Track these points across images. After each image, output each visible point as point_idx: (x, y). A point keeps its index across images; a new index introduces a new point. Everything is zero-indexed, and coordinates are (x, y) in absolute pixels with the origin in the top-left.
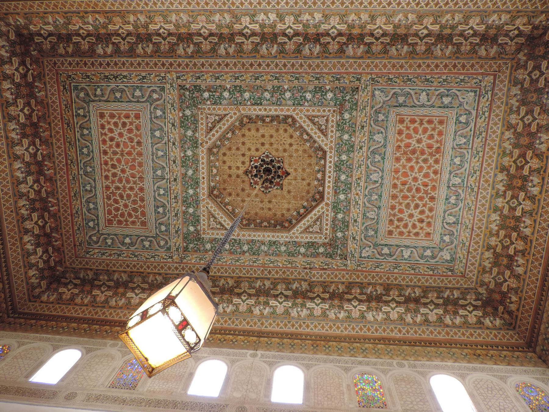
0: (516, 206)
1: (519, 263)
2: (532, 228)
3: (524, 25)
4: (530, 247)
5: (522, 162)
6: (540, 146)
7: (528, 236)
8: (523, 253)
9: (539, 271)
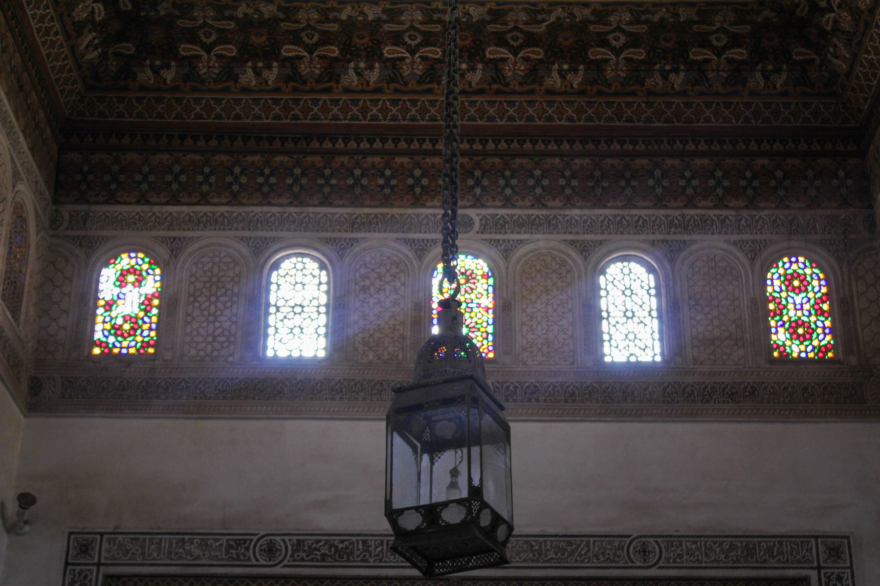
0: (405, 43)
1: (265, 73)
2: (360, 87)
3: (835, 22)
4: (312, 91)
5: (515, 39)
6: (555, 74)
7: (338, 82)
8: (292, 76)
9: (260, 118)
